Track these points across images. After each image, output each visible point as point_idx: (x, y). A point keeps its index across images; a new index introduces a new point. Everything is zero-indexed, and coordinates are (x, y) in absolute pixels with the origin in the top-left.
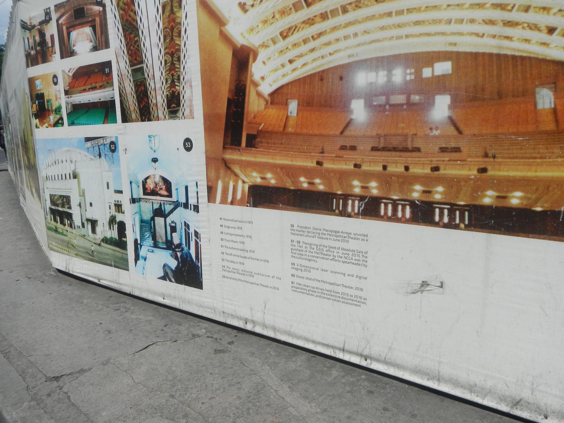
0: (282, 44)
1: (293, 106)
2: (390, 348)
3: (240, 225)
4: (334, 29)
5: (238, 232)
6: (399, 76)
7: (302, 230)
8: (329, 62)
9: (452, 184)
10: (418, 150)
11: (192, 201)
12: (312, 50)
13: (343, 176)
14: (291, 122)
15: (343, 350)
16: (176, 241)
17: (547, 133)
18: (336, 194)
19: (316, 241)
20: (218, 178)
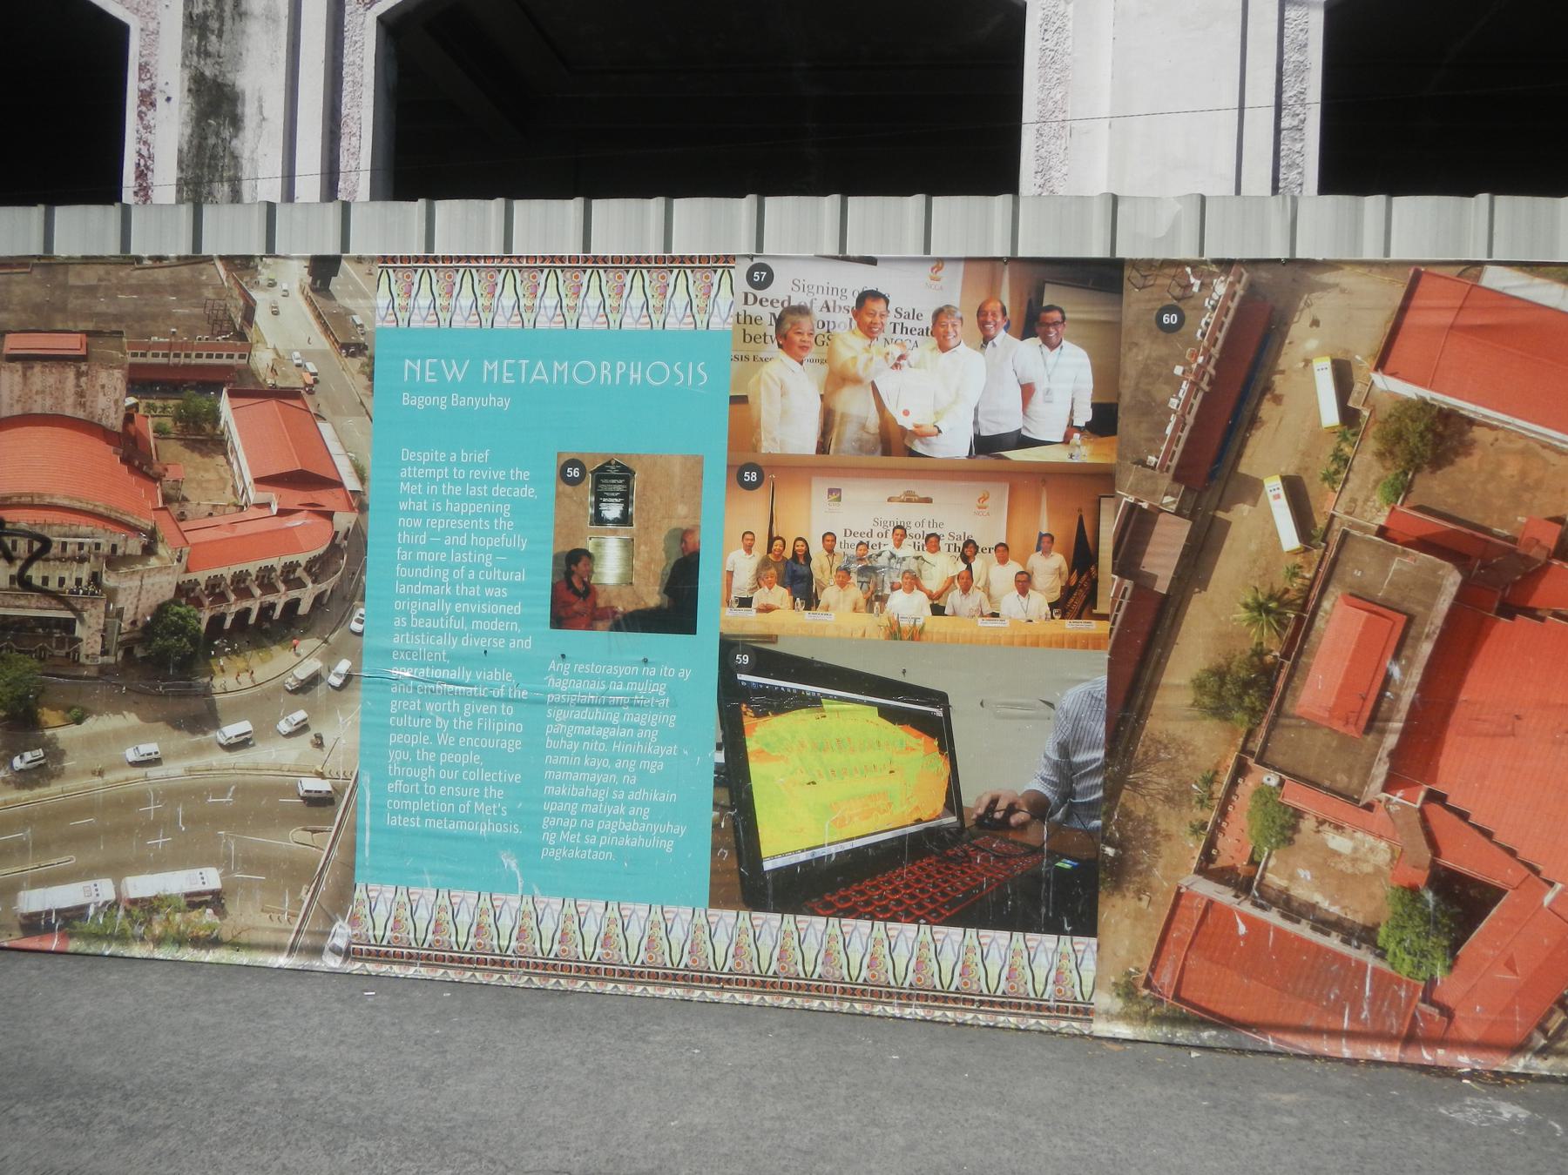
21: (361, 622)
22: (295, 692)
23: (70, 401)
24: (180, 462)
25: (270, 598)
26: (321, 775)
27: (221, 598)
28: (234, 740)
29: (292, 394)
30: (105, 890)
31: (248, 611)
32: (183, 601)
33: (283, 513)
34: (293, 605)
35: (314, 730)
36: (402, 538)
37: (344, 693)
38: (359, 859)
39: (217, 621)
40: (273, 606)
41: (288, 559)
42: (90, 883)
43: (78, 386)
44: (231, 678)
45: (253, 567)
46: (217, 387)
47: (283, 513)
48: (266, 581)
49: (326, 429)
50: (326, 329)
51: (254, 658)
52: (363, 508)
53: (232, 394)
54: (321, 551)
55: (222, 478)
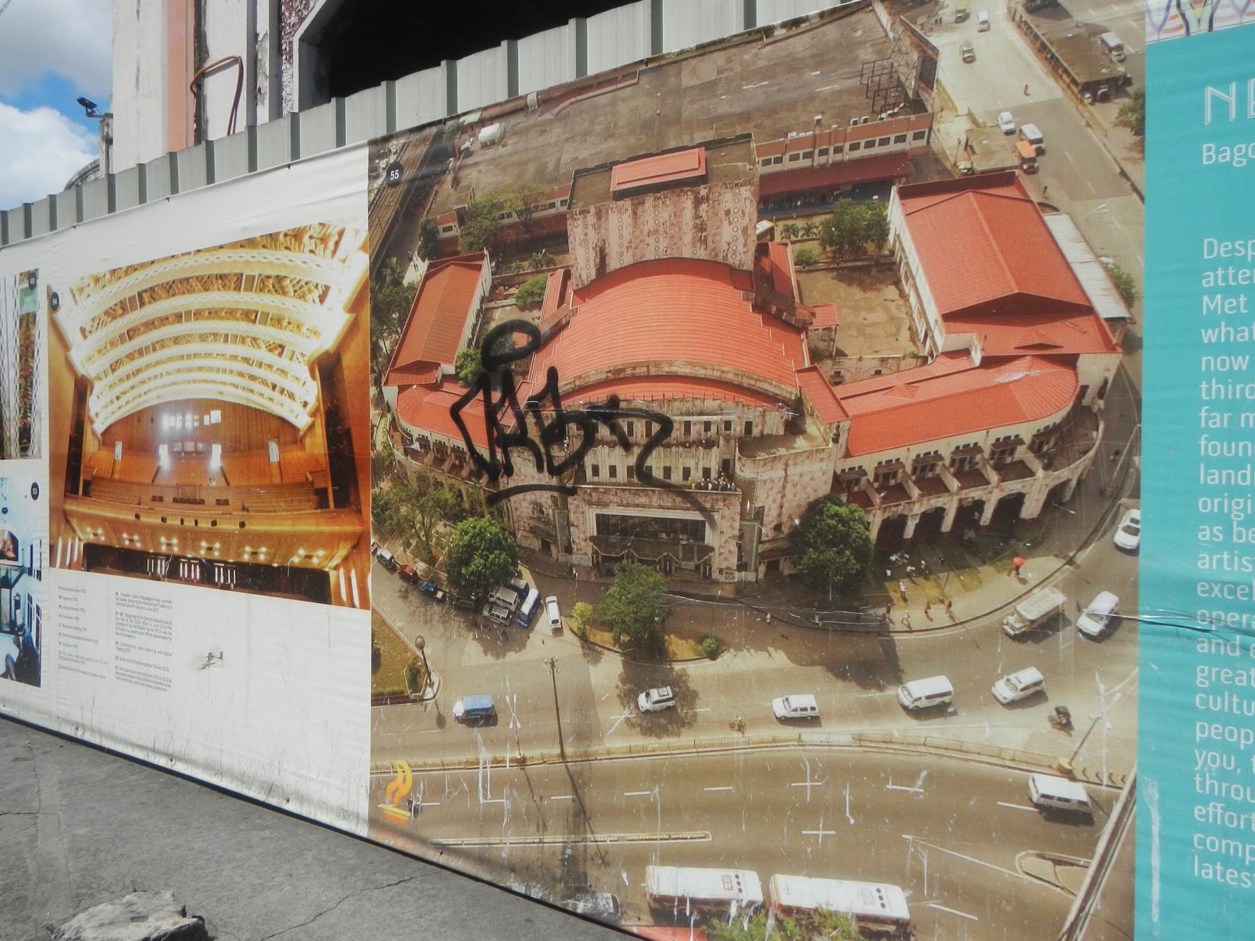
0: (112, 377)
1: (119, 448)
2: (188, 741)
3: (74, 595)
4: (148, 366)
5: (73, 604)
6: (190, 421)
7: (122, 599)
8: (145, 402)
9: (225, 537)
10: (202, 502)
11: (36, 566)
12: (132, 388)
13: (154, 531)
14: (117, 468)
15: (154, 751)
16: (19, 622)
17: (275, 486)
18: (148, 553)
19: (134, 612)
20: (59, 535)
21: (1135, 532)
22: (1020, 638)
23: (688, 238)
24: (832, 302)
25: (975, 493)
26: (1069, 774)
27: (899, 492)
28: (924, 703)
29: (1002, 178)
30: (749, 886)
31: (939, 513)
32: (844, 498)
33: (989, 362)
34: (1012, 504)
35: (1056, 699)
36: (1210, 390)
37: (1106, 647)
38: (1140, 922)
39: (893, 527)
40: (979, 505)
41: (1001, 433)
42: (732, 872)
43: (697, 217)
44: (916, 611)
45: (945, 447)
46: (881, 187)
47: (989, 362)
48: (966, 466)
49: (1059, 225)
50: (1055, 66)
51: (952, 583)
52: (1131, 345)
53: (905, 194)
54: (1056, 418)
55: (892, 319)
